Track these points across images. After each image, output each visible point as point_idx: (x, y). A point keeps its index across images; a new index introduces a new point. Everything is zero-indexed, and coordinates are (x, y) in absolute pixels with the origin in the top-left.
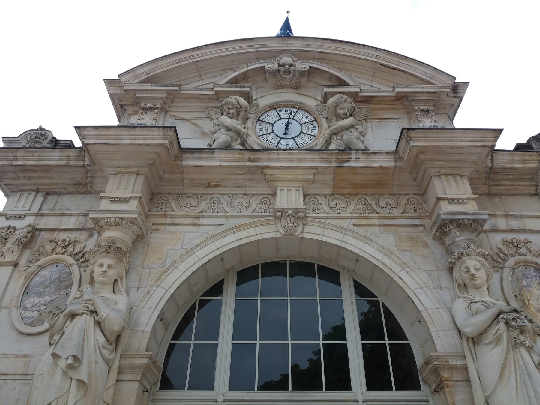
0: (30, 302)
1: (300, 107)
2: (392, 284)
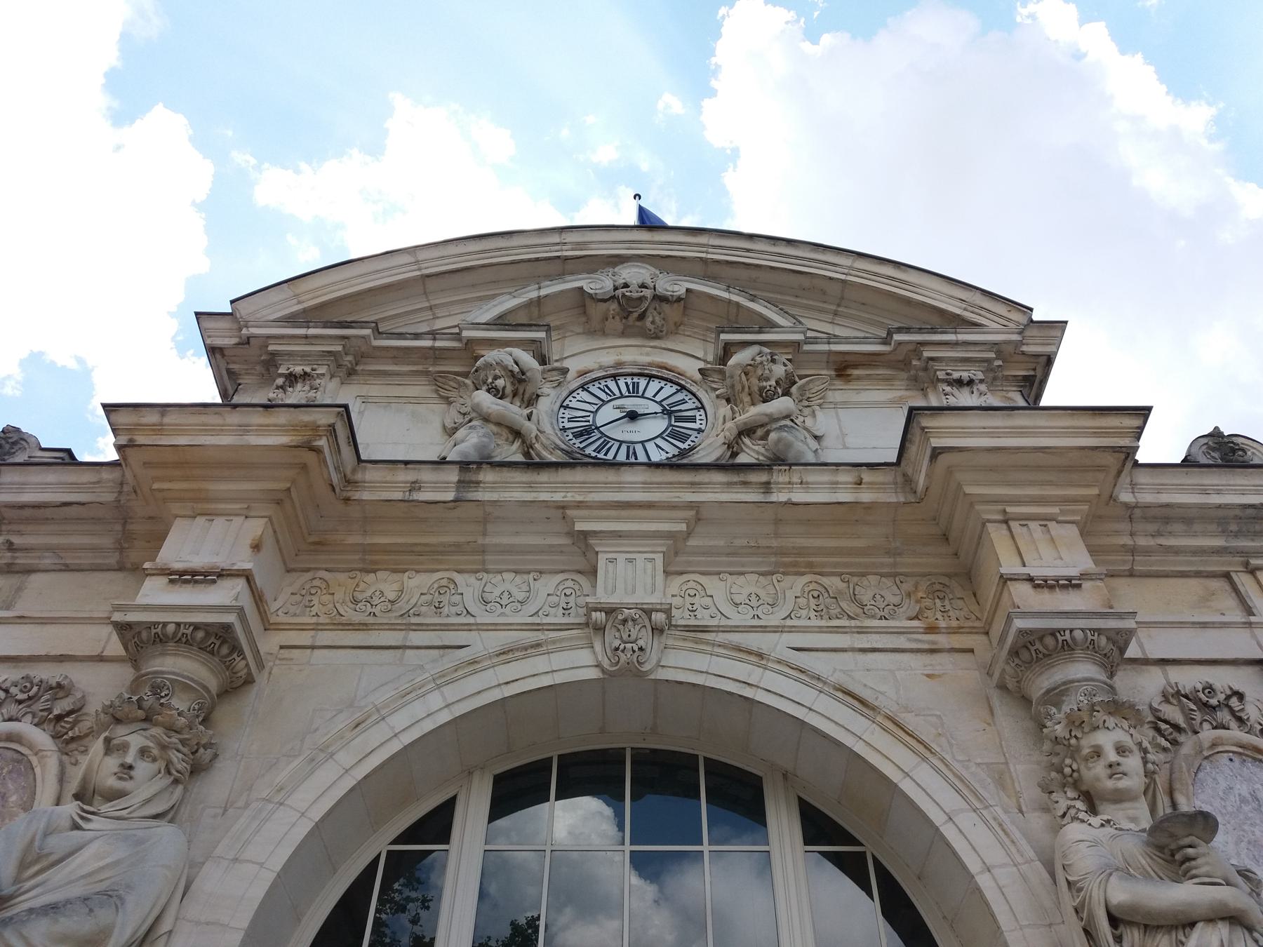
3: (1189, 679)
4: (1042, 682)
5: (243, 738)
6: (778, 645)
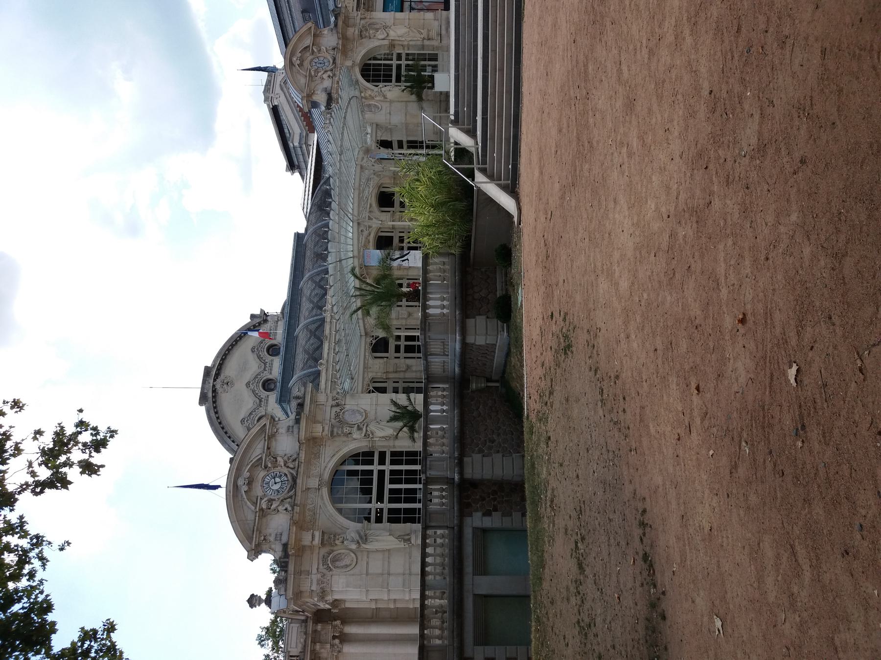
1: (312, 60)
3: (333, 416)
4: (335, 434)
6: (323, 465)
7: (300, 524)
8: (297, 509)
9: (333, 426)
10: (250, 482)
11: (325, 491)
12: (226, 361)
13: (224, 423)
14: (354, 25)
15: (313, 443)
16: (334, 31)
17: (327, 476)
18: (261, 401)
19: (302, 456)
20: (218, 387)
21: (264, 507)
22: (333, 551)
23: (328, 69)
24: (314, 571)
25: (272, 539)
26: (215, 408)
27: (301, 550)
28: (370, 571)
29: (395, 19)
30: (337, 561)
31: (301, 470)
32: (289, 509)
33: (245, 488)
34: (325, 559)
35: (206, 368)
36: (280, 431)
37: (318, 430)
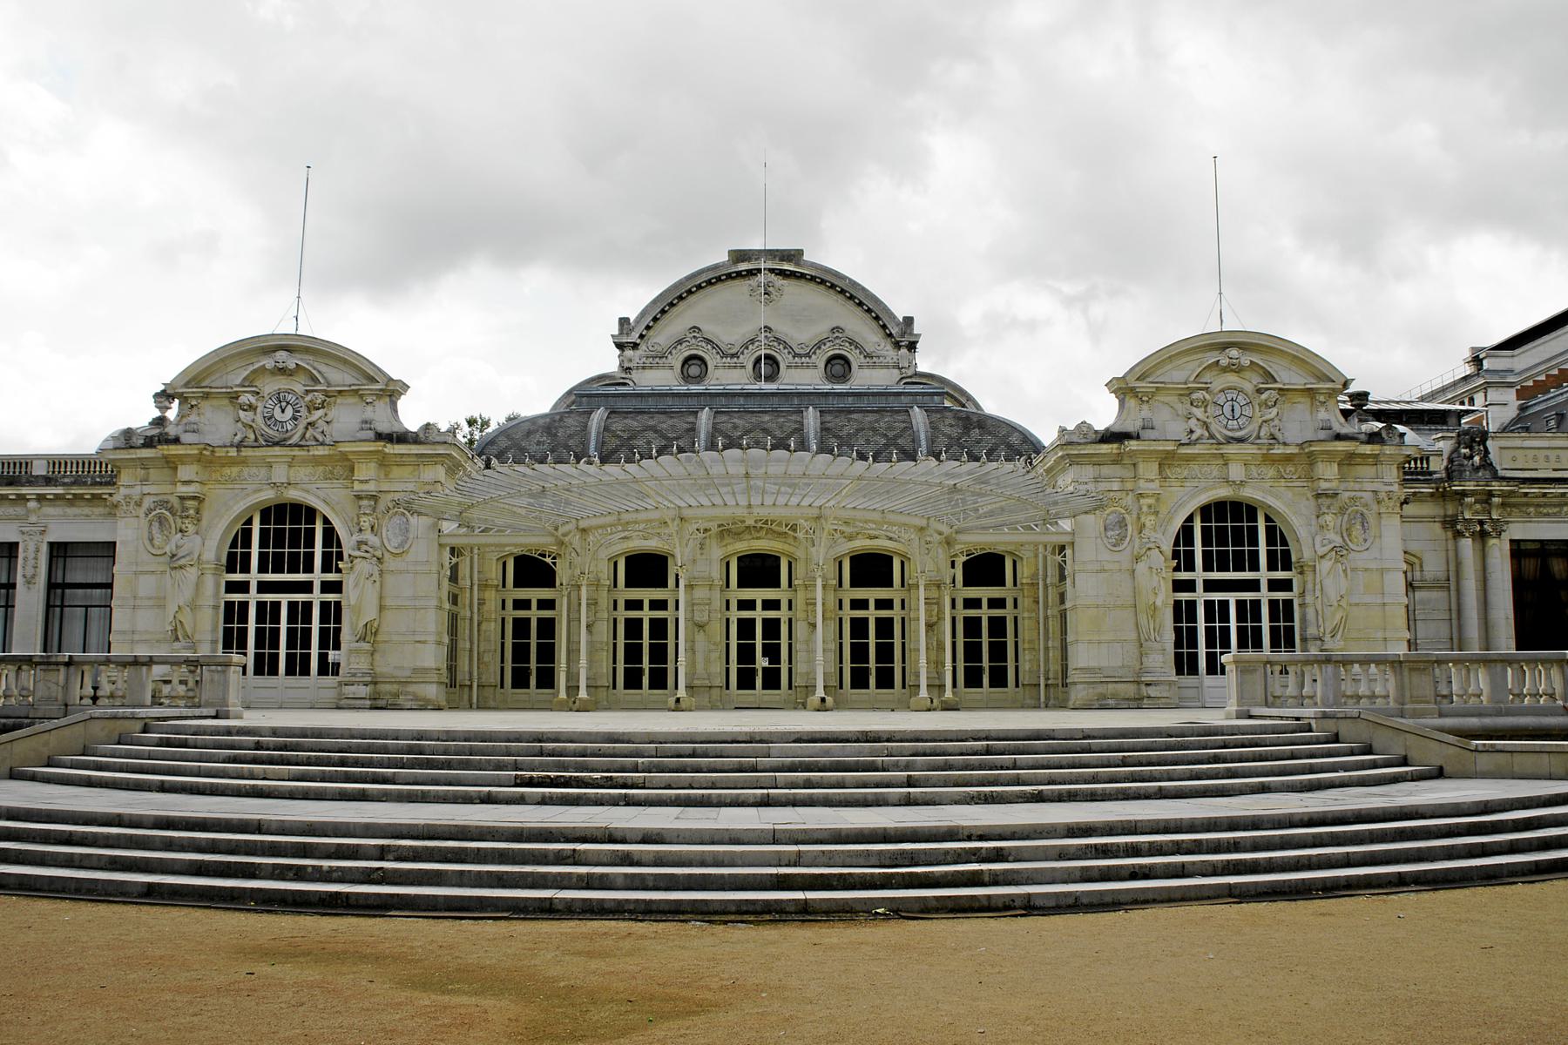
0: (1110, 533)
1: (1241, 391)
2: (1285, 521)
3: (396, 496)
5: (206, 515)
7: (207, 458)
8: (233, 452)
9: (374, 498)
10: (282, 371)
11: (268, 496)
12: (812, 285)
13: (692, 298)
14: (1343, 478)
15: (345, 466)
16: (1322, 435)
17: (294, 495)
18: (733, 356)
19: (321, 451)
20: (762, 278)
21: (244, 399)
22: (174, 515)
23: (1215, 427)
24: (146, 490)
25: (193, 418)
26: (719, 279)
27: (171, 464)
28: (142, 578)
29: (1382, 571)
30: (160, 523)
31: (296, 452)
32: (238, 438)
33: (268, 363)
34: (164, 504)
35: (800, 252)
36: (369, 408)
37: (365, 471)
